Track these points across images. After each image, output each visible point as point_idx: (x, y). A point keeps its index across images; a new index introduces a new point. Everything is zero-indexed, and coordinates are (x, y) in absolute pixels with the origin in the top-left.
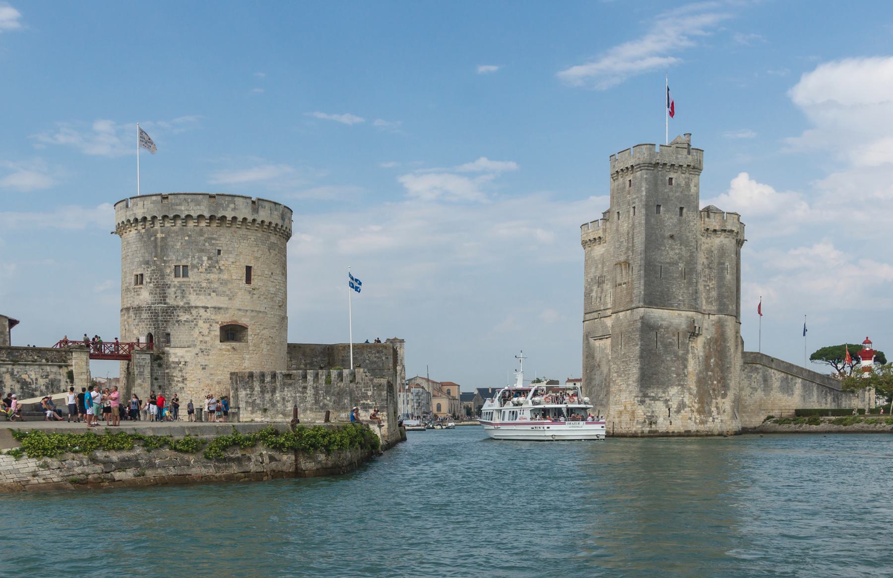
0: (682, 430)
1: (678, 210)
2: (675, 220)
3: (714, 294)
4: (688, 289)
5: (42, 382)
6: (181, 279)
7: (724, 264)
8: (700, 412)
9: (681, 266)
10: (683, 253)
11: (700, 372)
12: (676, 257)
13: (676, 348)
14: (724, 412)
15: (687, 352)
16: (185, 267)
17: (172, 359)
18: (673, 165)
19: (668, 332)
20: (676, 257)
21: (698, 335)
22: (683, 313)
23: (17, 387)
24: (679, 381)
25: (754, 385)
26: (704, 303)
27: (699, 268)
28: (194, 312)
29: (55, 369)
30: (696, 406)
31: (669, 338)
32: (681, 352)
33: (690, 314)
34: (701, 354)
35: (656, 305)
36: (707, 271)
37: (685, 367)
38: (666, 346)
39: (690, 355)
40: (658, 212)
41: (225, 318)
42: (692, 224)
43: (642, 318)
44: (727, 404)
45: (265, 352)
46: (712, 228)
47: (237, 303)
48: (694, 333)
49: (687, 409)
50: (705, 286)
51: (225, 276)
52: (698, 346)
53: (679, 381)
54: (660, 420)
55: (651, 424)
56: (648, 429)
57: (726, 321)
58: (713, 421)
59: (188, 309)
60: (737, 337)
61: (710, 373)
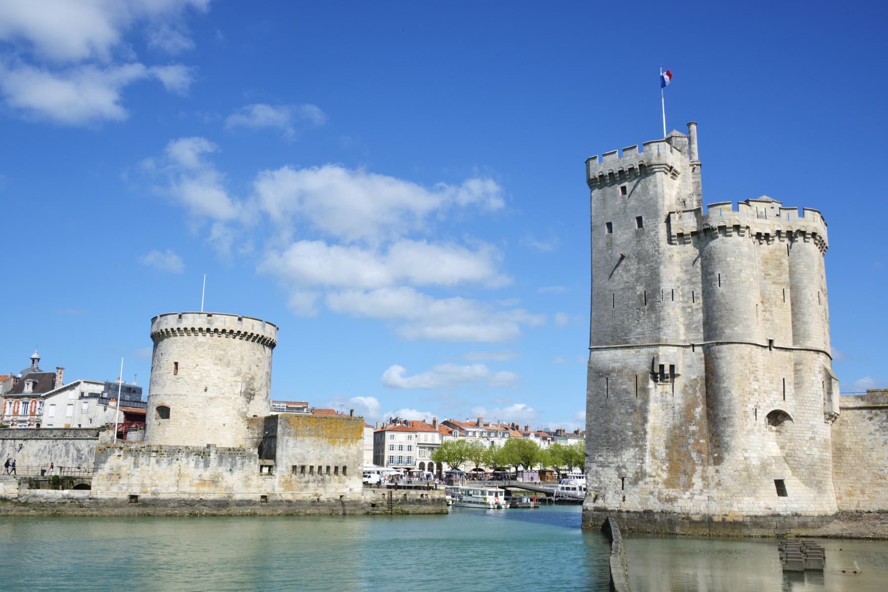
0: (640, 508)
3: (700, 316)
5: (87, 449)
7: (713, 273)
8: (669, 484)
9: (640, 289)
12: (632, 280)
13: (633, 395)
15: (646, 401)
24: (637, 440)
26: (682, 330)
30: (665, 476)
32: (639, 402)
33: (652, 350)
34: (679, 401)
35: (607, 343)
36: (687, 288)
37: (645, 420)
40: (610, 231)
42: (652, 234)
43: (589, 362)
46: (687, 231)
49: (648, 479)
50: (684, 308)
53: (637, 440)
54: (610, 495)
55: (596, 499)
57: (719, 352)
58: (691, 498)
60: (796, 371)
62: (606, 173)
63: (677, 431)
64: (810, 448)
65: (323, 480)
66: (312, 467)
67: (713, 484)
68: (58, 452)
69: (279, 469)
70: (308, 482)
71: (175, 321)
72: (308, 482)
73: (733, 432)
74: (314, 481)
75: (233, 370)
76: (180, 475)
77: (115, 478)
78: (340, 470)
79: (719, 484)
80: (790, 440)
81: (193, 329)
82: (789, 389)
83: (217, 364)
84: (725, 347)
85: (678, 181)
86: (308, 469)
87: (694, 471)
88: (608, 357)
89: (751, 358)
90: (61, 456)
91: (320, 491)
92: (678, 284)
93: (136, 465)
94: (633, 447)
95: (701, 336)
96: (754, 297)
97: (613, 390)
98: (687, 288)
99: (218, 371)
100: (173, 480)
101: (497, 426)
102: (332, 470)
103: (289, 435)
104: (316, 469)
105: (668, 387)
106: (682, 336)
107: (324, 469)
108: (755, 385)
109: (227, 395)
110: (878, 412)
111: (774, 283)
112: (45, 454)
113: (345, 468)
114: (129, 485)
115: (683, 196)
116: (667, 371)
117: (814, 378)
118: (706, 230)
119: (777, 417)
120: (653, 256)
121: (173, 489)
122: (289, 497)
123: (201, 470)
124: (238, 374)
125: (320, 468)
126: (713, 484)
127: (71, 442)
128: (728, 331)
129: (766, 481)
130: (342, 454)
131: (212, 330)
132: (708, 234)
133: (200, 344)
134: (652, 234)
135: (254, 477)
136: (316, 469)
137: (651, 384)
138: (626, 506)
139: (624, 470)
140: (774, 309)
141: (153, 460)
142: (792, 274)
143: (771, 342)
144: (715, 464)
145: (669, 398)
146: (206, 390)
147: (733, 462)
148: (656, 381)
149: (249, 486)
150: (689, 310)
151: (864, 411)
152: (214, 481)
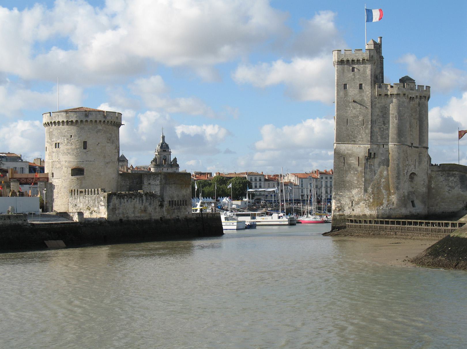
0: (361, 214)
1: (358, 85)
2: (357, 90)
9: (361, 118)
13: (357, 166)
16: (58, 143)
20: (357, 113)
21: (374, 157)
25: (451, 184)
26: (379, 138)
28: (62, 163)
30: (371, 200)
31: (351, 160)
36: (381, 119)
38: (350, 165)
41: (74, 165)
44: (394, 198)
50: (380, 128)
54: (346, 208)
56: (338, 213)
60: (419, 156)
61: (383, 180)
70: (174, 209)
72: (174, 209)
76: (134, 208)
80: (416, 185)
83: (108, 143)
87: (384, 198)
88: (345, 148)
91: (179, 214)
93: (120, 203)
94: (357, 188)
96: (408, 127)
97: (347, 163)
110: (444, 172)
114: (119, 214)
116: (372, 156)
121: (133, 215)
122: (169, 218)
130: (185, 194)
138: (354, 213)
139: (352, 198)
141: (126, 200)
142: (420, 114)
151: (440, 172)
152: (145, 211)
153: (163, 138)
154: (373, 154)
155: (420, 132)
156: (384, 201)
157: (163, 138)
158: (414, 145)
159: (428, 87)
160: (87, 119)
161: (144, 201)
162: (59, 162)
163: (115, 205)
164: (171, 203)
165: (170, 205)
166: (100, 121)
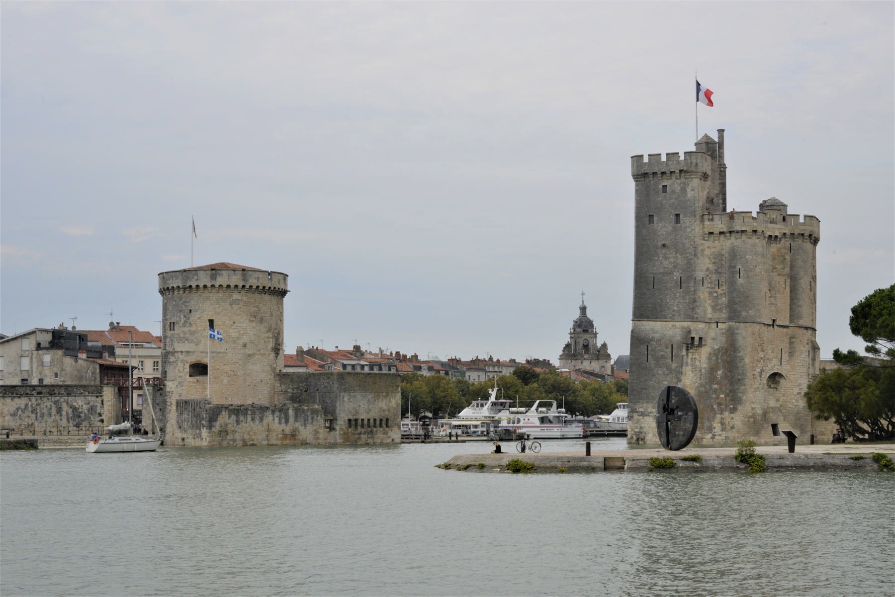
1: (673, 217)
3: (724, 300)
4: (684, 298)
6: (172, 332)
7: (735, 267)
9: (677, 275)
10: (679, 261)
11: (701, 385)
12: (671, 266)
14: (733, 428)
17: (168, 389)
18: (663, 173)
19: (660, 345)
22: (678, 324)
23: (70, 410)
26: (709, 310)
27: (700, 275)
29: (94, 398)
33: (686, 324)
36: (714, 277)
38: (657, 359)
39: (689, 368)
41: (193, 359)
42: (689, 230)
43: (632, 332)
45: (225, 382)
46: (716, 231)
47: (201, 347)
48: (692, 343)
50: (710, 293)
51: (193, 329)
52: (702, 357)
57: (737, 329)
58: (713, 438)
59: (173, 353)
60: (791, 343)
61: (716, 386)
62: (650, 171)
63: (703, 389)
64: (797, 401)
65: (371, 431)
66: (362, 420)
67: (728, 428)
68: (45, 411)
69: (339, 422)
70: (360, 434)
71: (209, 277)
72: (360, 434)
73: (745, 389)
74: (365, 434)
75: (265, 327)
76: (269, 430)
77: (223, 434)
78: (384, 422)
79: (733, 428)
81: (228, 286)
82: (785, 356)
83: (252, 321)
84: (742, 325)
85: (709, 183)
86: (360, 422)
87: (714, 418)
89: (759, 334)
90: (50, 415)
92: (707, 273)
93: (238, 422)
95: (723, 316)
96: (764, 287)
98: (714, 277)
99: (254, 327)
100: (264, 435)
101: (376, 355)
102: (378, 422)
103: (345, 391)
104: (366, 422)
105: (696, 356)
106: (709, 313)
107: (372, 421)
108: (762, 355)
109: (262, 351)
111: (779, 275)
112: (28, 413)
113: (387, 420)
115: (712, 195)
116: (696, 343)
117: (802, 348)
118: (730, 232)
119: (775, 378)
120: (689, 248)
123: (283, 426)
124: (269, 330)
125: (369, 420)
126: (728, 428)
127: (62, 400)
128: (744, 314)
129: (766, 425)
130: (385, 408)
131: (247, 287)
132: (733, 235)
133: (236, 302)
134: (689, 230)
135: (321, 431)
136: (366, 422)
137: (684, 353)
140: (778, 295)
142: (792, 267)
143: (774, 321)
144: (731, 413)
145: (697, 363)
146: (245, 345)
147: (745, 410)
148: (687, 350)
149: (318, 439)
150: (715, 295)
153: (583, 309)
154: (697, 339)
155: (792, 299)
156: (715, 425)
157: (583, 309)
158: (778, 323)
159: (812, 219)
160: (213, 283)
161: (291, 419)
162: (173, 353)
163: (226, 425)
164: (353, 423)
165: (350, 427)
166: (236, 286)
